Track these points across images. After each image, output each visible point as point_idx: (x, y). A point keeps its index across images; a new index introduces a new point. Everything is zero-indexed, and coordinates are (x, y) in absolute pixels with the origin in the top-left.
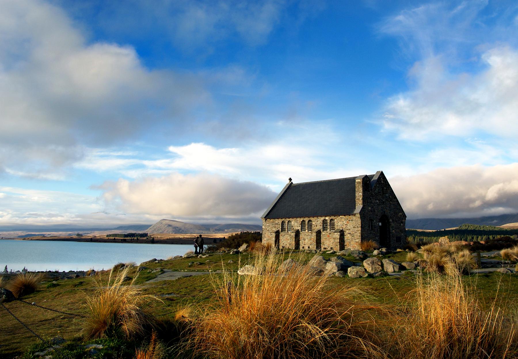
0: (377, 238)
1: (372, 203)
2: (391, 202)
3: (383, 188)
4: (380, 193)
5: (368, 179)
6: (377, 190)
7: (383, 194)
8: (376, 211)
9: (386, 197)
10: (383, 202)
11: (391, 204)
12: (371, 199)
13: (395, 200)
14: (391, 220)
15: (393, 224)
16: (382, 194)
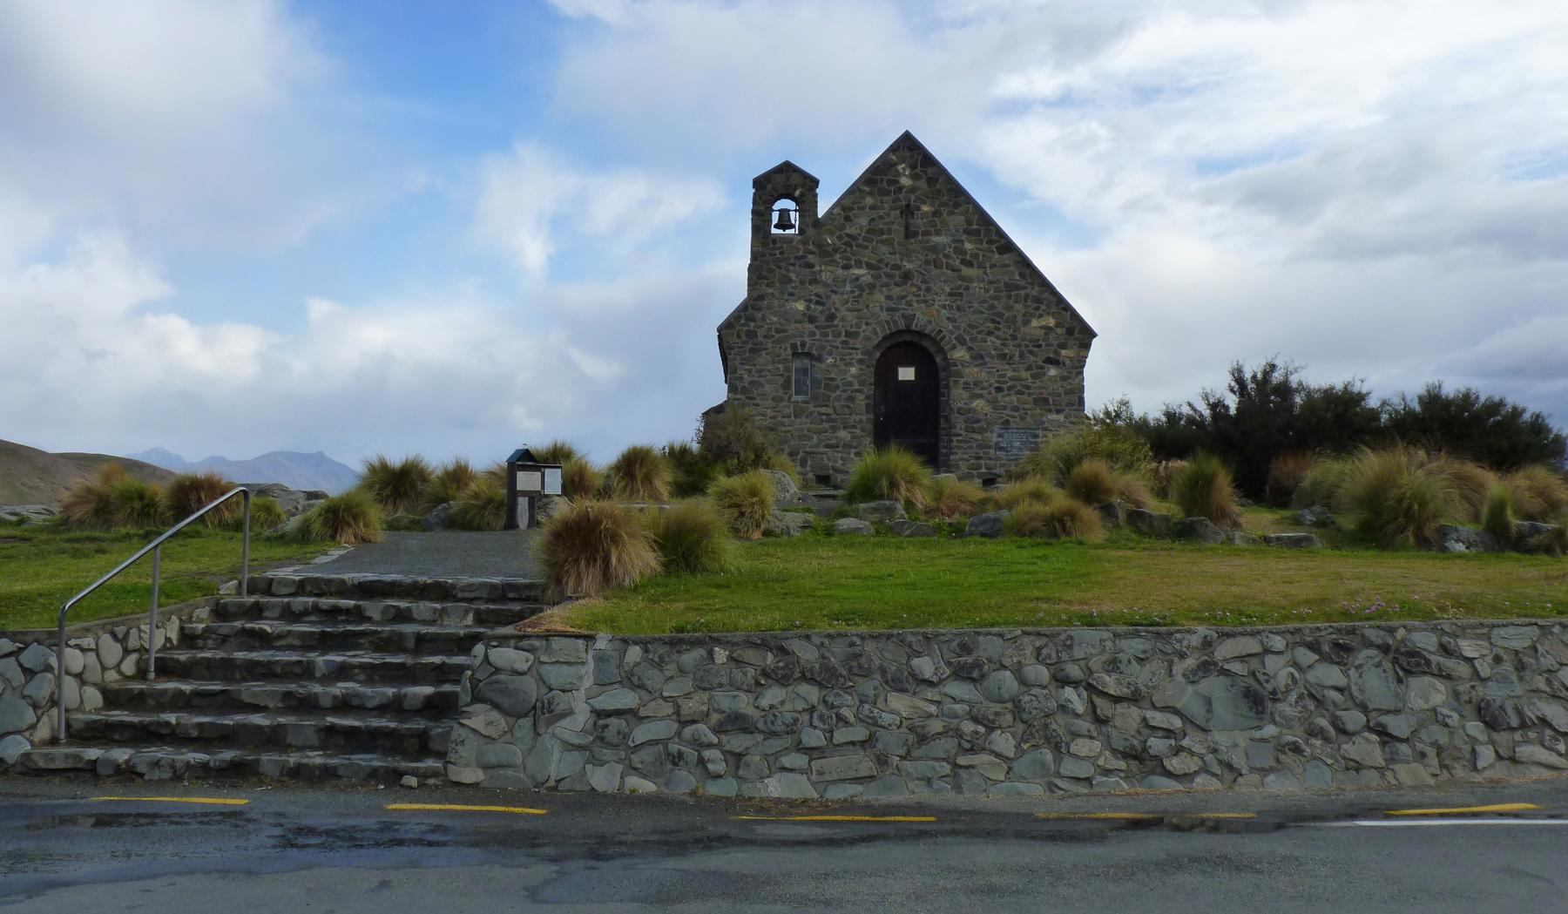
0: (843, 435)
1: (814, 281)
2: (966, 271)
3: (908, 211)
4: (882, 232)
5: (795, 179)
6: (864, 221)
7: (909, 234)
8: (843, 312)
9: (934, 249)
10: (907, 276)
11: (962, 279)
12: (812, 266)
13: (1007, 258)
14: (960, 354)
15: (972, 372)
16: (898, 233)
